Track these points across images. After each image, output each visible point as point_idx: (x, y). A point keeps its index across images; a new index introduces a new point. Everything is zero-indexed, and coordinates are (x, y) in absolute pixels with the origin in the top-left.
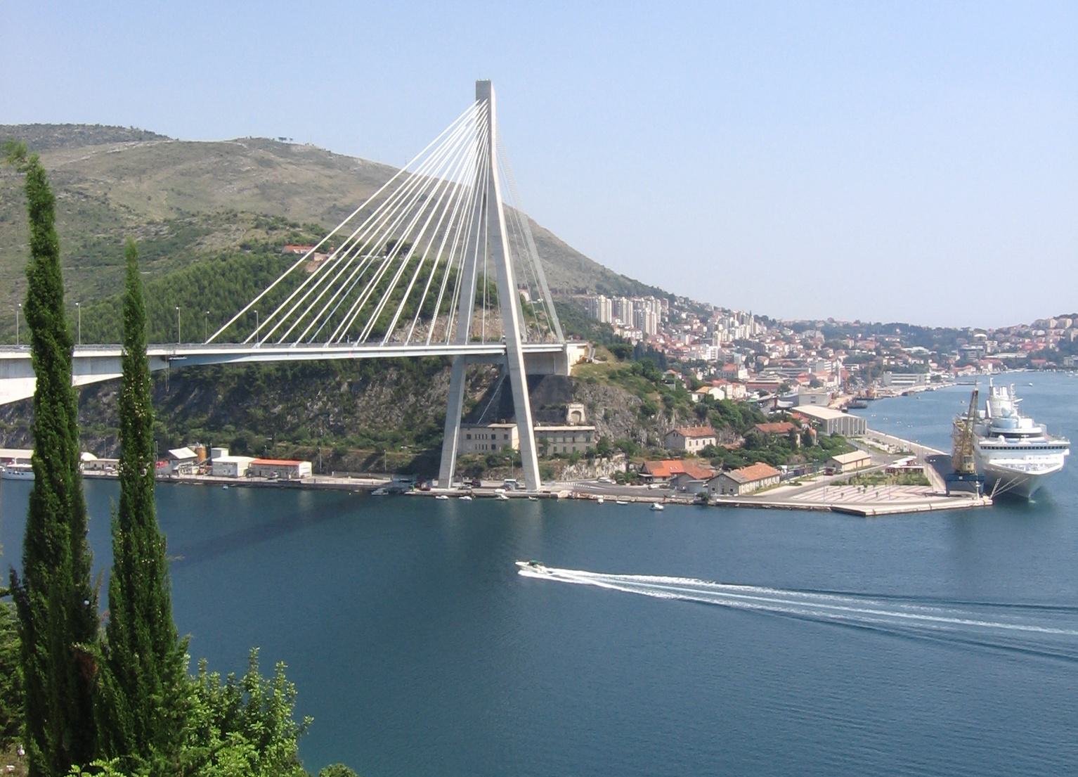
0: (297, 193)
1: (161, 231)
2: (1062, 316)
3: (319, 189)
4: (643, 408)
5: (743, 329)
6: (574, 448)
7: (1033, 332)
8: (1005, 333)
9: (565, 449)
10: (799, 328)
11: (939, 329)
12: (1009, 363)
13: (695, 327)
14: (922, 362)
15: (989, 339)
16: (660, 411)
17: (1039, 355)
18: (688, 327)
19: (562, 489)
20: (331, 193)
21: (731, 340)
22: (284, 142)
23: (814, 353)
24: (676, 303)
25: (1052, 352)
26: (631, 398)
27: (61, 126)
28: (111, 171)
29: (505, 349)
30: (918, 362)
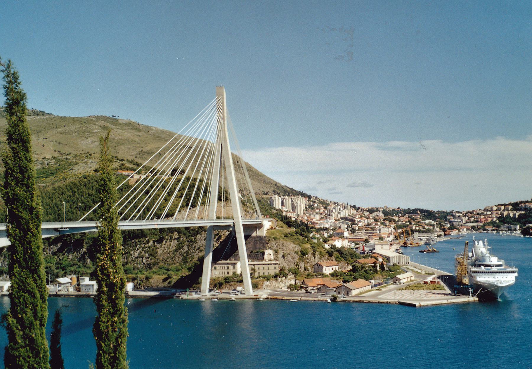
2: (499, 205)
3: (134, 142)
4: (301, 251)
5: (345, 212)
6: (269, 273)
8: (471, 213)
9: (264, 273)
10: (371, 211)
11: (438, 211)
12: (473, 228)
13: (322, 211)
15: (463, 216)
16: (310, 253)
17: (489, 224)
18: (318, 211)
19: (263, 294)
20: (140, 144)
21: (339, 217)
23: (379, 223)
24: (311, 199)
25: (495, 222)
26: (295, 247)
29: (234, 222)
30: (430, 228)
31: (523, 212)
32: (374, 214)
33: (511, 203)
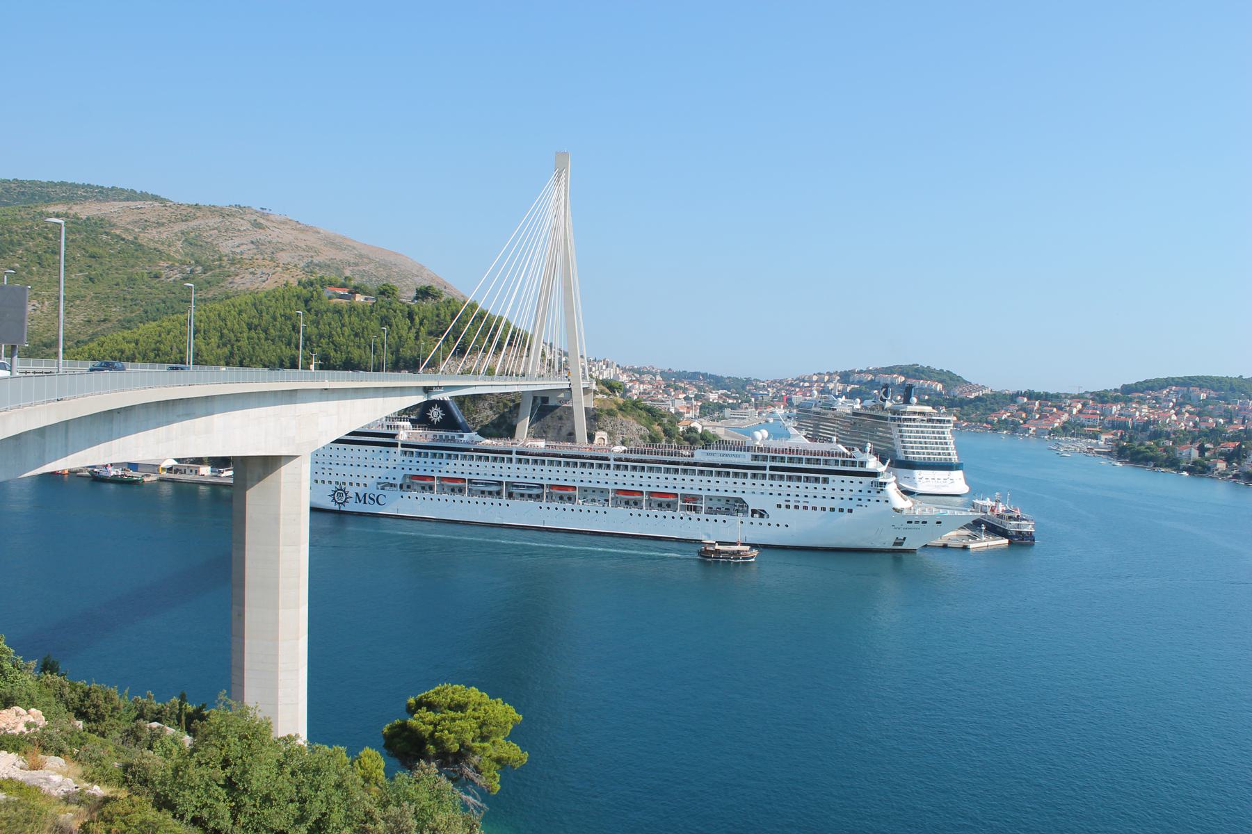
0: (283, 250)
1: (197, 271)
4: (650, 436)
7: (801, 384)
8: (781, 382)
10: (640, 372)
11: (729, 378)
14: (735, 402)
22: (264, 211)
27: (83, 186)
28: (136, 222)
29: (570, 384)
31: (856, 386)
32: (647, 378)
33: (837, 372)
